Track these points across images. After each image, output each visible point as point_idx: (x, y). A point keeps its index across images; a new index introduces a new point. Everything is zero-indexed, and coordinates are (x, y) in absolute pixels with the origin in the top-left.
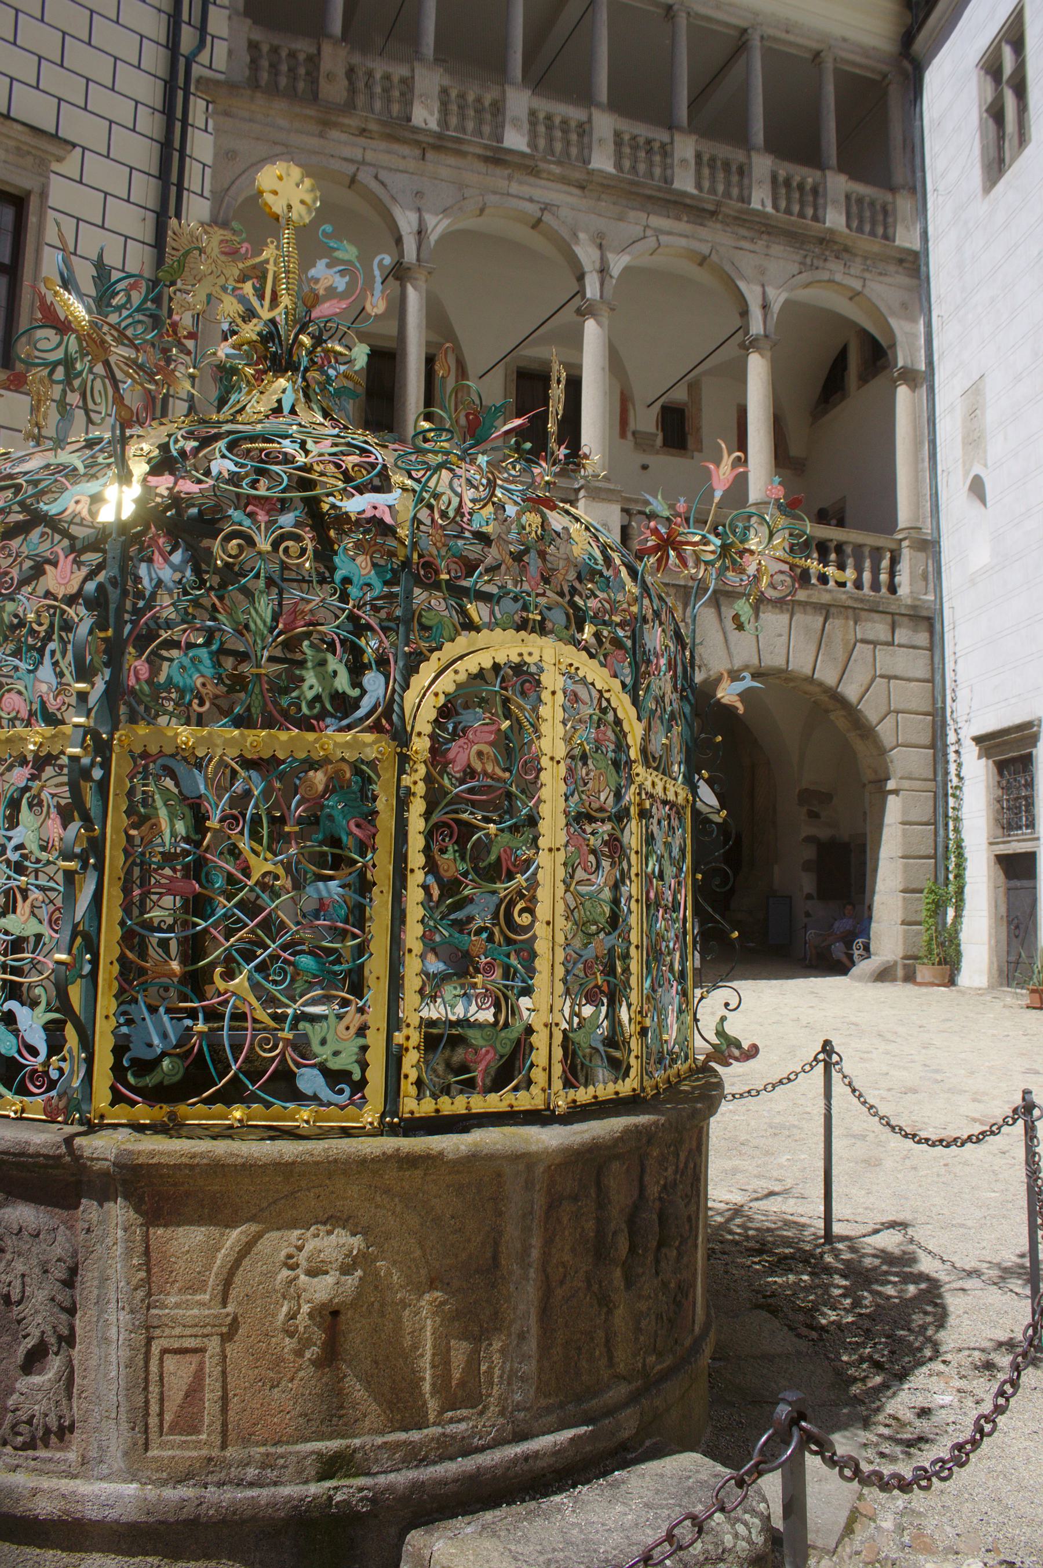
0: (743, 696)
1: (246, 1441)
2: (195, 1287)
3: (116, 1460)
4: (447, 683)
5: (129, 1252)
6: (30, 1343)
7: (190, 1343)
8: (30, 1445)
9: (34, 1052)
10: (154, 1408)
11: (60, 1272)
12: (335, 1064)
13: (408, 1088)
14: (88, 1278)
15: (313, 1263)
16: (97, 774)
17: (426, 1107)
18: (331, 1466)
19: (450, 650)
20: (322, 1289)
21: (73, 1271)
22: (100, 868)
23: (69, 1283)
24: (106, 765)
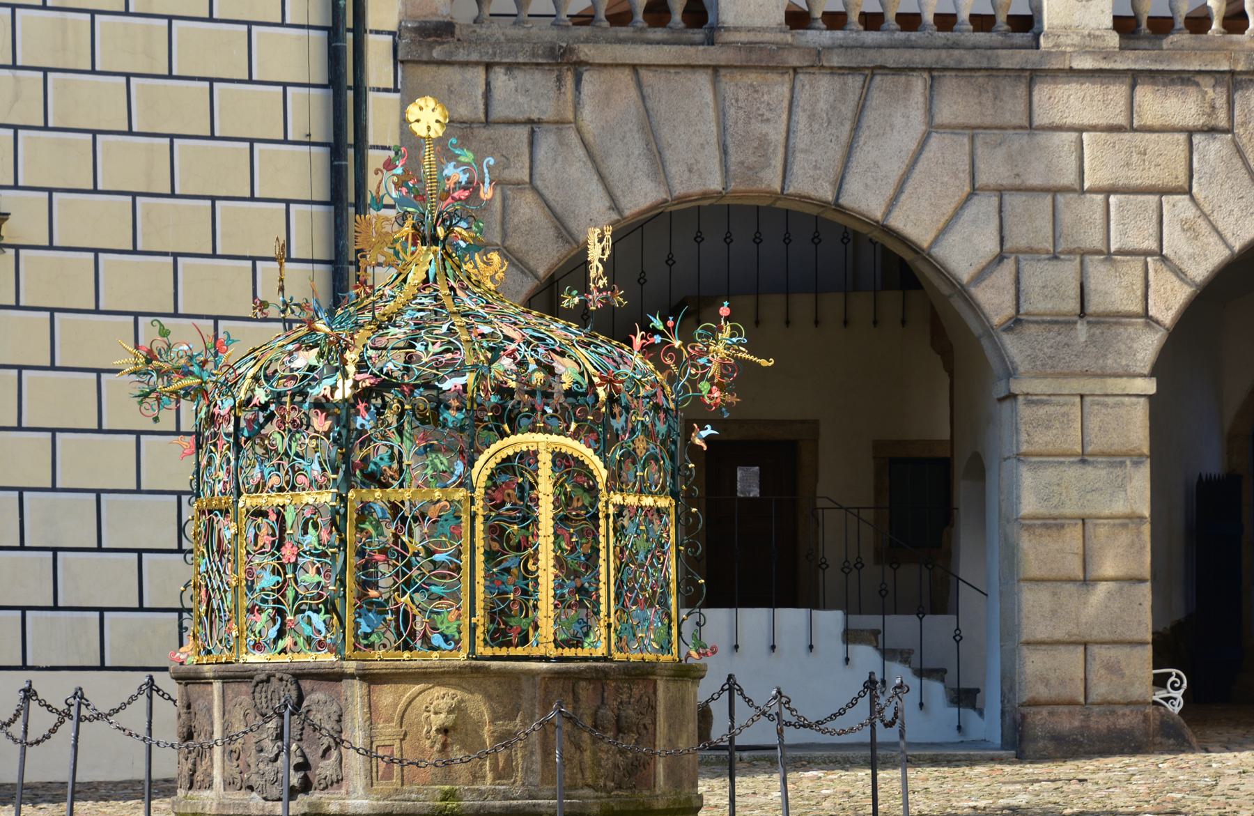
0: (707, 440)
1: (411, 783)
2: (388, 721)
3: (361, 792)
4: (492, 464)
5: (363, 706)
6: (324, 747)
7: (388, 743)
8: (326, 788)
9: (319, 632)
10: (374, 769)
11: (335, 717)
12: (447, 632)
13: (479, 642)
14: (347, 719)
15: (436, 704)
16: (342, 511)
17: (488, 652)
18: (447, 796)
19: (494, 448)
20: (438, 720)
21: (340, 716)
22: (345, 550)
23: (339, 721)
24: (346, 507)
